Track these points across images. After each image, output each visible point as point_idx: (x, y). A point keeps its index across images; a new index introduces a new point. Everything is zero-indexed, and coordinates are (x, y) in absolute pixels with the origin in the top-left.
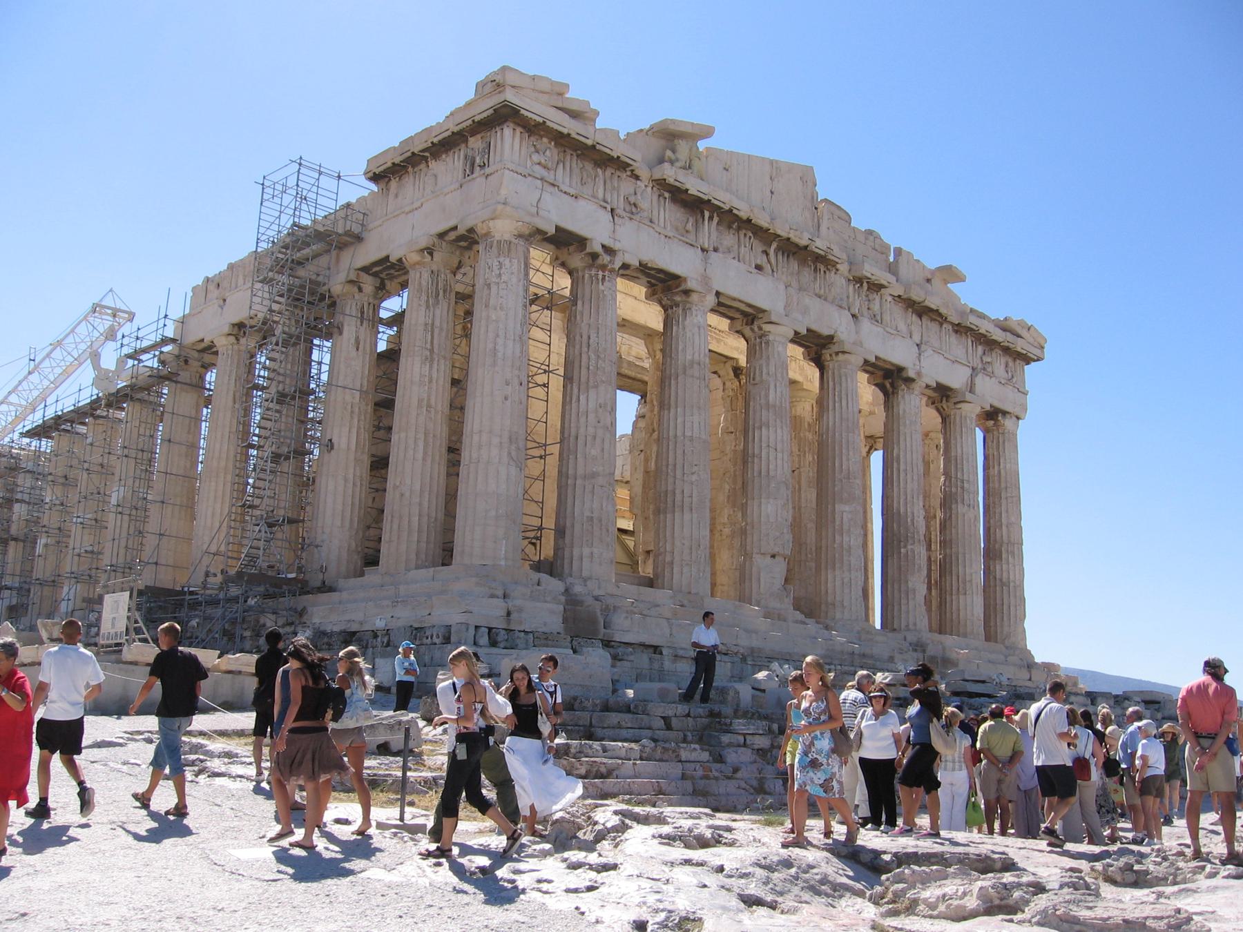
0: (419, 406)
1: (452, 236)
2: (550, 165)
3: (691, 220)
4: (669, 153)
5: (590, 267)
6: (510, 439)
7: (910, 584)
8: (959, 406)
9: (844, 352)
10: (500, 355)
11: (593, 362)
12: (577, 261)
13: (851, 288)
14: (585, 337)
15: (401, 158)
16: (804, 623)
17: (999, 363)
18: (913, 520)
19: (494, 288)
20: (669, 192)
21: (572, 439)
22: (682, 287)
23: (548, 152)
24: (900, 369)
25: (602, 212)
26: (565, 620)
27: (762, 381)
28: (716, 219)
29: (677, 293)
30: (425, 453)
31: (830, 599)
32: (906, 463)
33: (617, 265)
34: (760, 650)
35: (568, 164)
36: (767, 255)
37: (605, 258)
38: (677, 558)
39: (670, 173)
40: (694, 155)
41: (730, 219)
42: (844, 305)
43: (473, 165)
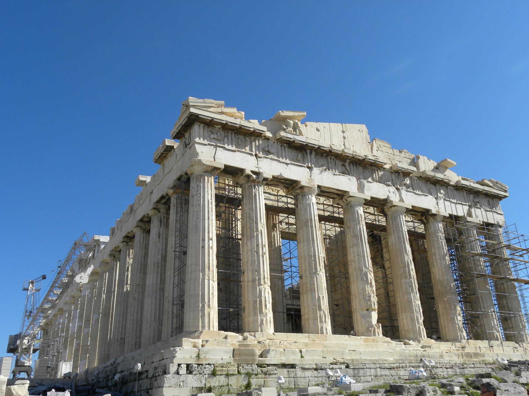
2: (220, 139)
3: (300, 155)
5: (248, 181)
9: (394, 206)
12: (242, 180)
13: (393, 176)
15: (163, 150)
19: (195, 197)
20: (286, 143)
23: (219, 133)
24: (428, 211)
28: (314, 153)
29: (297, 189)
34: (357, 360)
35: (230, 138)
36: (345, 166)
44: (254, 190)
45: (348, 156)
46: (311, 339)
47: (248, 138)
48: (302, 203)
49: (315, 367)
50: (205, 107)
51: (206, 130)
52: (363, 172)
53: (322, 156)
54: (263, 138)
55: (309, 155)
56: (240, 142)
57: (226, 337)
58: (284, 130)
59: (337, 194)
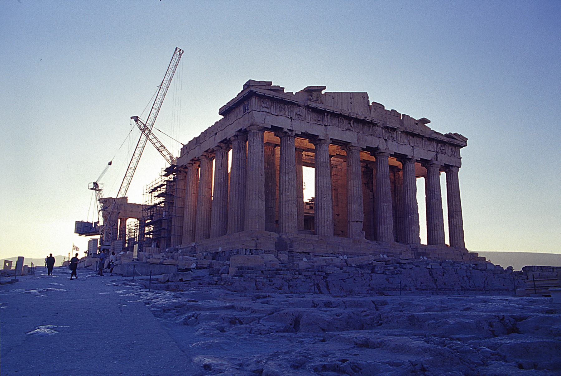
0: (236, 183)
4: (310, 97)
17: (448, 150)
33: (294, 134)
37: (290, 133)
38: (320, 225)
41: (333, 115)
58: (310, 100)
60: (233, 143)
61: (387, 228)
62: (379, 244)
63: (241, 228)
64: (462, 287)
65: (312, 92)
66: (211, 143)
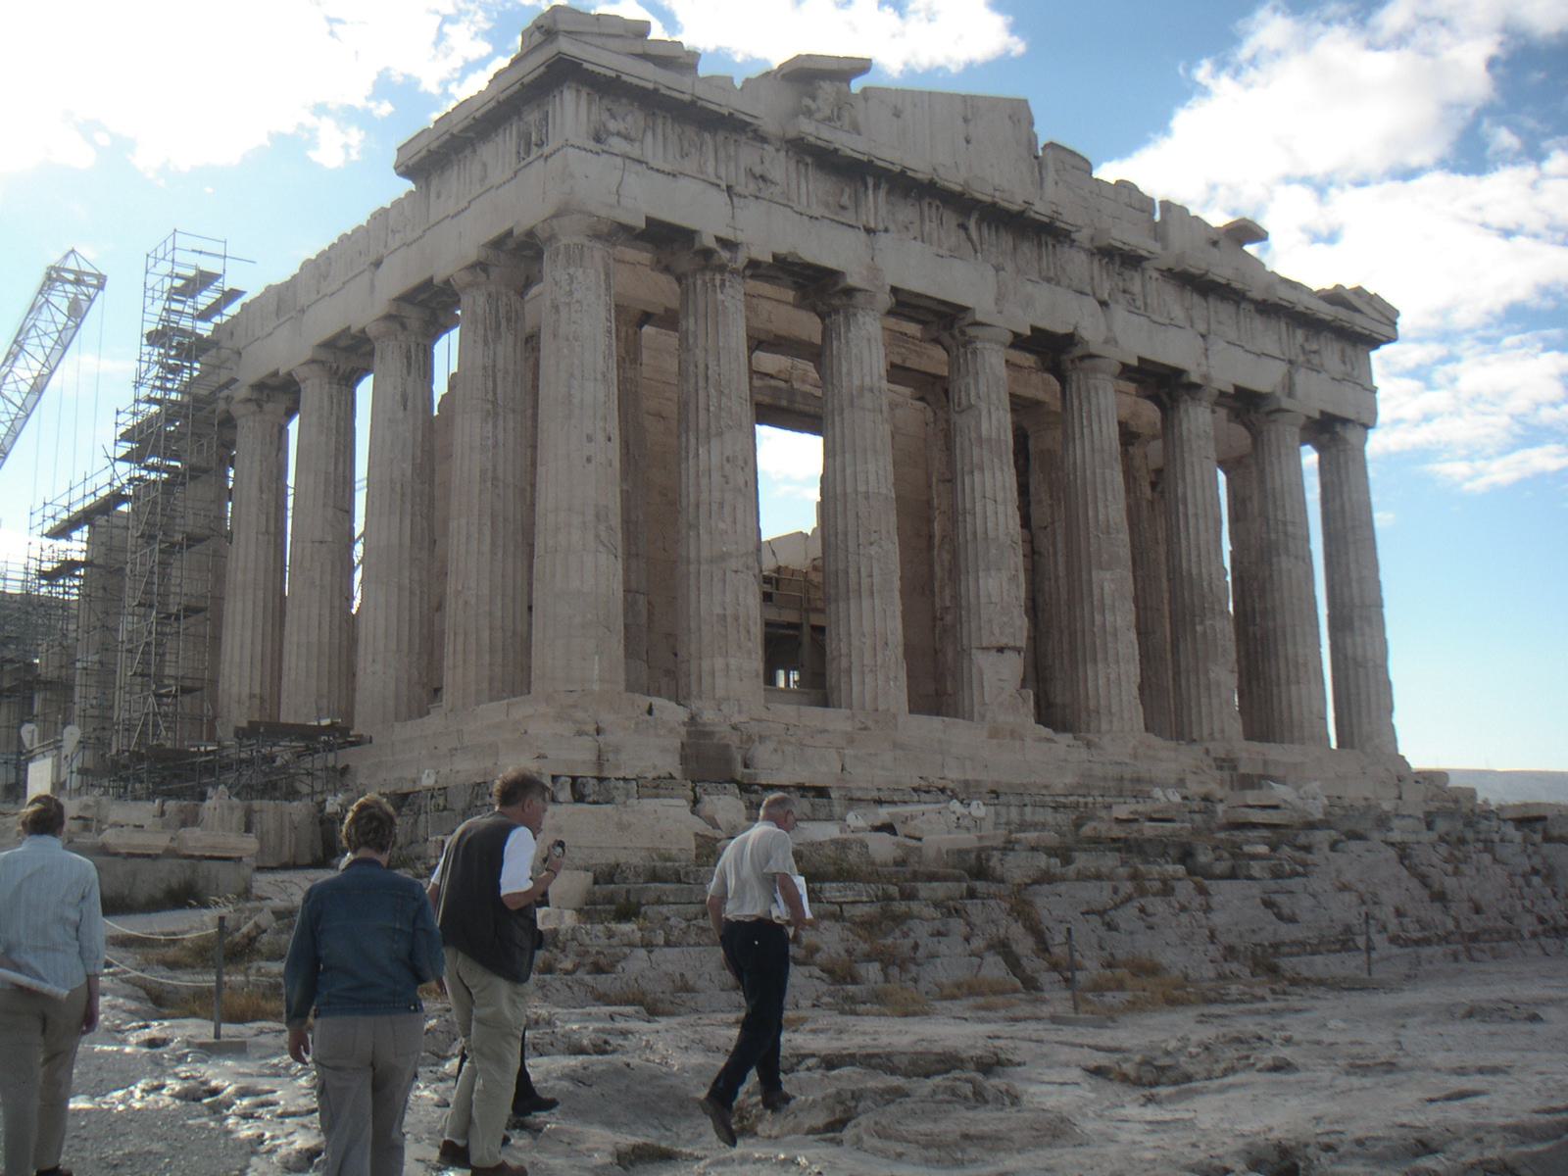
0: (483, 481)
1: (511, 244)
2: (633, 134)
4: (807, 101)
5: (703, 269)
6: (597, 516)
7: (1212, 675)
8: (1272, 418)
9: (1092, 356)
10: (576, 401)
11: (714, 401)
12: (685, 262)
14: (701, 367)
16: (1049, 740)
17: (1331, 353)
18: (1210, 584)
21: (691, 509)
22: (841, 285)
24: (1178, 372)
25: (713, 191)
26: (684, 759)
27: (970, 406)
28: (884, 187)
30: (493, 544)
31: (1092, 704)
32: (1196, 506)
33: (741, 261)
34: (978, 783)
35: (659, 131)
37: (725, 255)
39: (808, 128)
40: (844, 102)
41: (905, 186)
42: (1088, 290)
43: (528, 144)
44: (720, 297)
45: (979, 202)
46: (860, 725)
47: (707, 136)
48: (847, 338)
49: (875, 794)
50: (601, 35)
51: (594, 109)
52: (1015, 248)
53: (906, 195)
54: (750, 134)
55: (870, 192)
56: (686, 145)
57: (650, 711)
58: (809, 113)
59: (936, 313)
60: (466, 300)
61: (1114, 675)
62: (1089, 745)
63: (516, 674)
64: (1541, 920)
65: (812, 78)
66: (361, 307)
